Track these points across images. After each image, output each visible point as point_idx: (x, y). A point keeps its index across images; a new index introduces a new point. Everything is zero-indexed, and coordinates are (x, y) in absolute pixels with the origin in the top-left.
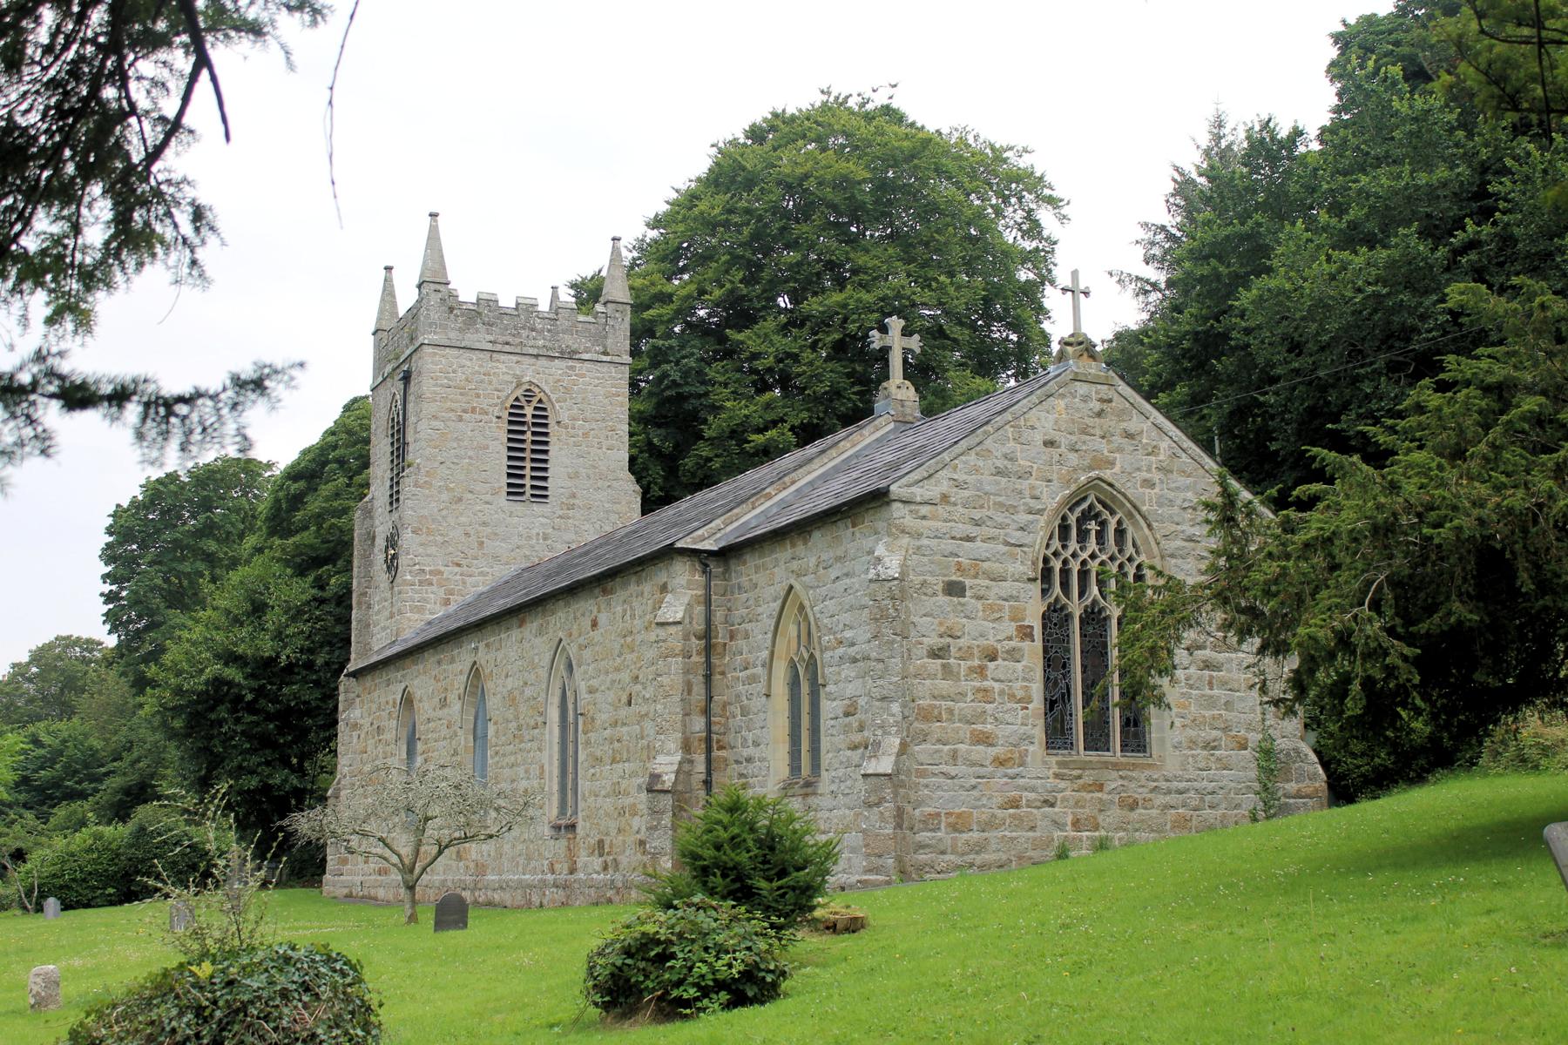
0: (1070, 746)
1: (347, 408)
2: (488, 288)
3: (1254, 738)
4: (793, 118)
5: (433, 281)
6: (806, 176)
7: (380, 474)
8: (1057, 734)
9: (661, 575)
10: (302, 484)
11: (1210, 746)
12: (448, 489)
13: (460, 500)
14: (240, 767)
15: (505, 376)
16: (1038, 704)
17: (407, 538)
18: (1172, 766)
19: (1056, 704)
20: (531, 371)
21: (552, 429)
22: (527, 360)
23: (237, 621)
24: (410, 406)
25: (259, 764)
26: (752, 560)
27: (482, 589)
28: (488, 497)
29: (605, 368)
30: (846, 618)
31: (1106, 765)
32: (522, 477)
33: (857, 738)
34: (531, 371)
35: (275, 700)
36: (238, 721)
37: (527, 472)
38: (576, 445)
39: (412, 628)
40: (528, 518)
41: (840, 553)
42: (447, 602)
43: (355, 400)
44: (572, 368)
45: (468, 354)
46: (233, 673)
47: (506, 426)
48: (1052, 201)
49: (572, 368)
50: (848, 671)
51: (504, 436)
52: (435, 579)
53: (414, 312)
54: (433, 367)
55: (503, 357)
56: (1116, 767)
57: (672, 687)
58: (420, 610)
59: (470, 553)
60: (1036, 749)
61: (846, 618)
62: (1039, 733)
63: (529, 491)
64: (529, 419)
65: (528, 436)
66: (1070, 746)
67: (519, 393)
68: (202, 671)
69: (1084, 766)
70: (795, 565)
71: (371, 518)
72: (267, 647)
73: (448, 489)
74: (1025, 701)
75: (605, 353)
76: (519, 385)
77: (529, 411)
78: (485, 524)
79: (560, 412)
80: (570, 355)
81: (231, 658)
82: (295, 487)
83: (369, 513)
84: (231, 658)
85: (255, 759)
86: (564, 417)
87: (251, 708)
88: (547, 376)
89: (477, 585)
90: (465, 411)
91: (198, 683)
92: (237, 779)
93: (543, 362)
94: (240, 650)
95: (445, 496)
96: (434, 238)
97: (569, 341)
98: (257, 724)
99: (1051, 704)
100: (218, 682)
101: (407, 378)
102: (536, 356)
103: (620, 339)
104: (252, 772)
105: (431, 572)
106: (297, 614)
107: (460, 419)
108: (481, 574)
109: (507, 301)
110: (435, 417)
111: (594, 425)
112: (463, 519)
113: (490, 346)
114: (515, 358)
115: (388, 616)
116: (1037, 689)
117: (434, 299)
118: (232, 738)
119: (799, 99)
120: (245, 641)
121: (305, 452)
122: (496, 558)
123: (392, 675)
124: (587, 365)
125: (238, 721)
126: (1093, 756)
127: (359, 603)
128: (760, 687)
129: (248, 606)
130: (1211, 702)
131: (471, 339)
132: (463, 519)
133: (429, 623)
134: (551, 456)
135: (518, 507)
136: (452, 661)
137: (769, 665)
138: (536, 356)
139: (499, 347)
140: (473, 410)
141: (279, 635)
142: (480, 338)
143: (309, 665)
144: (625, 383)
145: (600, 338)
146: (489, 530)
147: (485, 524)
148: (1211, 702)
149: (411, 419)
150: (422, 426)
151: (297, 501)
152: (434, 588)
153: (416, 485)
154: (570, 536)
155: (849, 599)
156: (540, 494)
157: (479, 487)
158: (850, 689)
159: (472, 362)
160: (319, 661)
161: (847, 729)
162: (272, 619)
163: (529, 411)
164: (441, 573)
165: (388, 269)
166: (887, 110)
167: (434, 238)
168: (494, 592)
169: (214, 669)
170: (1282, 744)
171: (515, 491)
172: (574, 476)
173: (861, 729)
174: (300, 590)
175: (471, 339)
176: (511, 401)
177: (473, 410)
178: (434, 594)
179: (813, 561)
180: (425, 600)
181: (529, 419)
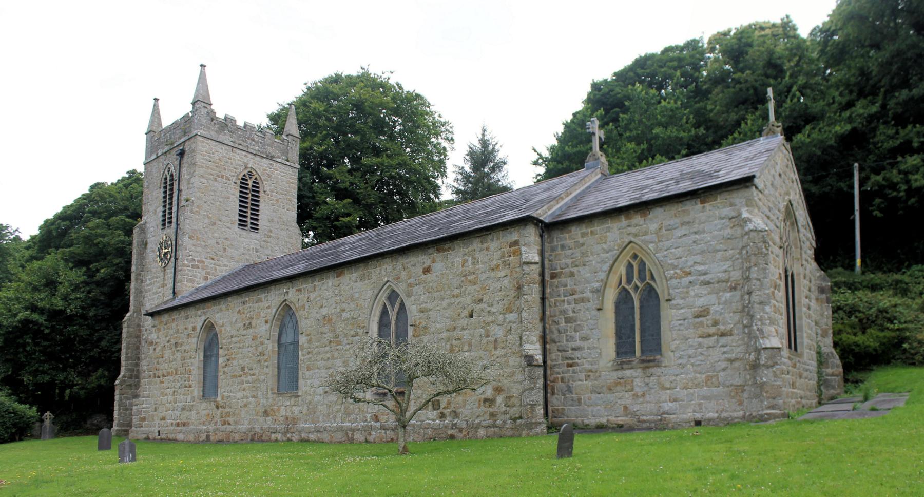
2: (232, 114)
7: (151, 209)
9: (514, 235)
10: (67, 223)
12: (209, 217)
13: (215, 224)
14: (37, 370)
15: (240, 162)
17: (185, 241)
20: (254, 163)
21: (261, 194)
22: (249, 155)
23: (36, 289)
25: (50, 369)
26: (576, 230)
27: (224, 274)
28: (229, 225)
29: (287, 168)
30: (698, 258)
32: (246, 217)
33: (712, 330)
34: (254, 163)
35: (61, 334)
36: (36, 344)
37: (249, 214)
38: (273, 205)
40: (248, 239)
41: (686, 219)
42: (206, 279)
43: (98, 184)
44: (272, 165)
46: (35, 317)
47: (239, 188)
49: (272, 165)
50: (704, 290)
51: (238, 194)
52: (200, 265)
53: (185, 125)
54: (204, 151)
55: (238, 151)
57: (534, 302)
58: (192, 281)
59: (220, 253)
61: (698, 258)
63: (249, 226)
64: (250, 187)
65: (250, 196)
67: (246, 172)
68: (15, 315)
70: (633, 230)
71: (144, 233)
72: (59, 303)
73: (209, 217)
75: (287, 160)
76: (246, 168)
77: (250, 183)
78: (227, 239)
79: (266, 186)
80: (271, 158)
81: (33, 308)
82: (64, 224)
83: (143, 230)
84: (33, 308)
85: (47, 366)
86: (267, 189)
87: (46, 337)
88: (260, 166)
89: (223, 271)
90: (218, 176)
91: (14, 321)
92: (35, 376)
93: (257, 158)
94: (41, 304)
95: (206, 221)
97: (270, 150)
98: (49, 346)
100: (26, 322)
102: (255, 155)
103: (294, 155)
104: (44, 372)
105: (198, 261)
106: (76, 288)
107: (215, 180)
108: (225, 265)
109: (240, 123)
111: (281, 196)
112: (216, 235)
113: (232, 144)
114: (244, 153)
115: (150, 288)
118: (34, 354)
120: (42, 299)
121: (66, 208)
122: (232, 258)
123: (199, 312)
124: (279, 165)
125: (36, 344)
127: (137, 279)
128: (593, 305)
129: (44, 281)
132: (216, 235)
133: (197, 289)
134: (261, 208)
135: (244, 233)
136: (259, 301)
137: (600, 292)
138: (255, 155)
139: (236, 146)
140: (222, 177)
141: (65, 298)
143: (84, 317)
144: (296, 177)
145: (285, 152)
146: (228, 242)
147: (227, 239)
150: (196, 181)
151: (64, 233)
152: (200, 270)
153: (191, 212)
154: (268, 252)
155: (697, 248)
156: (255, 227)
157: (224, 219)
158: (701, 302)
160: (91, 314)
161: (696, 326)
162: (62, 289)
163: (250, 183)
164: (203, 262)
168: (235, 275)
169: (21, 316)
171: (242, 223)
172: (271, 221)
173: (716, 323)
174: (78, 275)
176: (241, 176)
177: (222, 177)
178: (200, 274)
179: (653, 227)
180: (195, 276)
181: (250, 187)
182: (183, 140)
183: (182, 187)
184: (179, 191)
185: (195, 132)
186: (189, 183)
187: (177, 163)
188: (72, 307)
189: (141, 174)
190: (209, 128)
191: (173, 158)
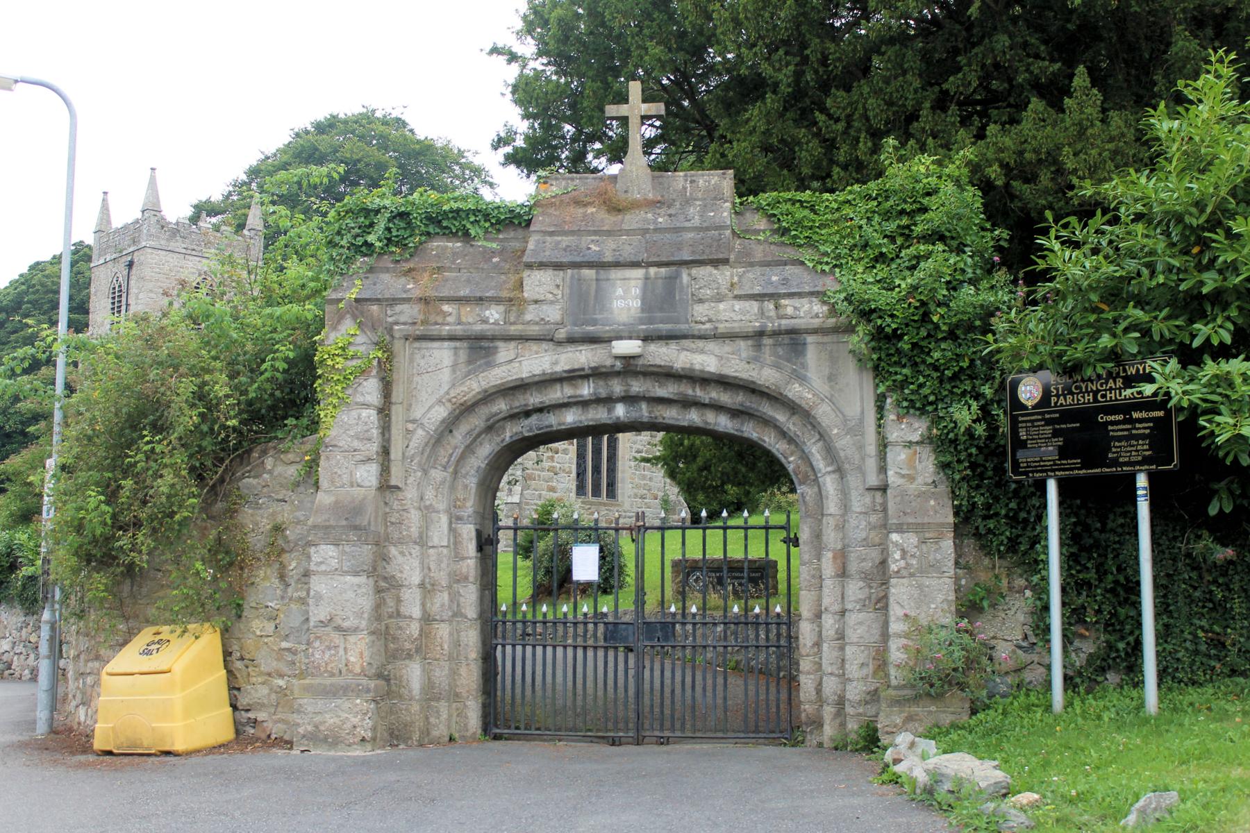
0: (585, 494)
1: (32, 268)
3: (661, 494)
4: (345, 122)
5: (152, 209)
6: (359, 161)
8: (581, 490)
11: (643, 497)
16: (574, 475)
18: (627, 506)
19: (581, 475)
24: (132, 283)
31: (600, 504)
39: (645, 436)
43: (38, 263)
45: (171, 255)
48: (491, 185)
56: (605, 505)
60: (573, 495)
62: (574, 488)
66: (585, 494)
69: (592, 504)
74: (570, 472)
96: (153, 183)
99: (578, 475)
101: (130, 265)
110: (151, 291)
116: (574, 467)
117: (153, 220)
119: (348, 108)
126: (595, 499)
130: (644, 477)
131: (173, 245)
142: (178, 245)
148: (644, 477)
149: (133, 291)
159: (173, 260)
165: (105, 193)
166: (398, 120)
167: (153, 183)
170: (672, 498)
175: (173, 245)
182: (131, 249)
183: (130, 302)
184: (127, 305)
185: (144, 244)
186: (137, 298)
187: (126, 273)
188: (11, 422)
189: (89, 247)
190: (158, 238)
191: (121, 269)
